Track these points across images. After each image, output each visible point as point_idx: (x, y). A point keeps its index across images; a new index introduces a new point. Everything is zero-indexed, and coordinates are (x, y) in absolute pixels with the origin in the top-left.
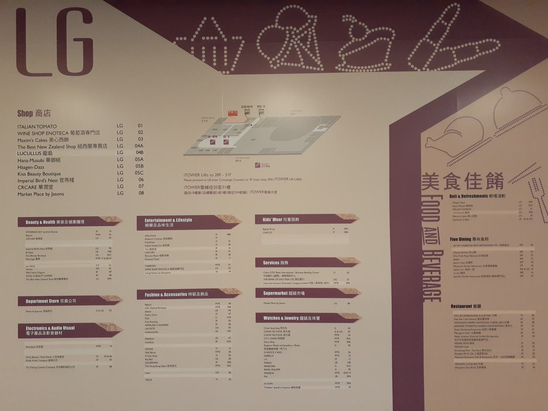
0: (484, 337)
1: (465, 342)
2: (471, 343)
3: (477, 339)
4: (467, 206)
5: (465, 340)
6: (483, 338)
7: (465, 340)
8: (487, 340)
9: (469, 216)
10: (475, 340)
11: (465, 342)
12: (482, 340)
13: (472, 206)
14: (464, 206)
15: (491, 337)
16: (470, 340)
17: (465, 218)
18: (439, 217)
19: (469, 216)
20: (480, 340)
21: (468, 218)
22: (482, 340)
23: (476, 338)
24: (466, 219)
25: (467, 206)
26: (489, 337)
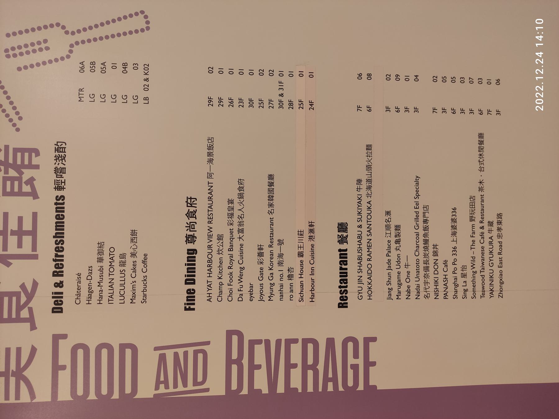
4: (100, 260)
13: (101, 245)
14: (101, 270)
18: (123, 347)
25: (100, 260)
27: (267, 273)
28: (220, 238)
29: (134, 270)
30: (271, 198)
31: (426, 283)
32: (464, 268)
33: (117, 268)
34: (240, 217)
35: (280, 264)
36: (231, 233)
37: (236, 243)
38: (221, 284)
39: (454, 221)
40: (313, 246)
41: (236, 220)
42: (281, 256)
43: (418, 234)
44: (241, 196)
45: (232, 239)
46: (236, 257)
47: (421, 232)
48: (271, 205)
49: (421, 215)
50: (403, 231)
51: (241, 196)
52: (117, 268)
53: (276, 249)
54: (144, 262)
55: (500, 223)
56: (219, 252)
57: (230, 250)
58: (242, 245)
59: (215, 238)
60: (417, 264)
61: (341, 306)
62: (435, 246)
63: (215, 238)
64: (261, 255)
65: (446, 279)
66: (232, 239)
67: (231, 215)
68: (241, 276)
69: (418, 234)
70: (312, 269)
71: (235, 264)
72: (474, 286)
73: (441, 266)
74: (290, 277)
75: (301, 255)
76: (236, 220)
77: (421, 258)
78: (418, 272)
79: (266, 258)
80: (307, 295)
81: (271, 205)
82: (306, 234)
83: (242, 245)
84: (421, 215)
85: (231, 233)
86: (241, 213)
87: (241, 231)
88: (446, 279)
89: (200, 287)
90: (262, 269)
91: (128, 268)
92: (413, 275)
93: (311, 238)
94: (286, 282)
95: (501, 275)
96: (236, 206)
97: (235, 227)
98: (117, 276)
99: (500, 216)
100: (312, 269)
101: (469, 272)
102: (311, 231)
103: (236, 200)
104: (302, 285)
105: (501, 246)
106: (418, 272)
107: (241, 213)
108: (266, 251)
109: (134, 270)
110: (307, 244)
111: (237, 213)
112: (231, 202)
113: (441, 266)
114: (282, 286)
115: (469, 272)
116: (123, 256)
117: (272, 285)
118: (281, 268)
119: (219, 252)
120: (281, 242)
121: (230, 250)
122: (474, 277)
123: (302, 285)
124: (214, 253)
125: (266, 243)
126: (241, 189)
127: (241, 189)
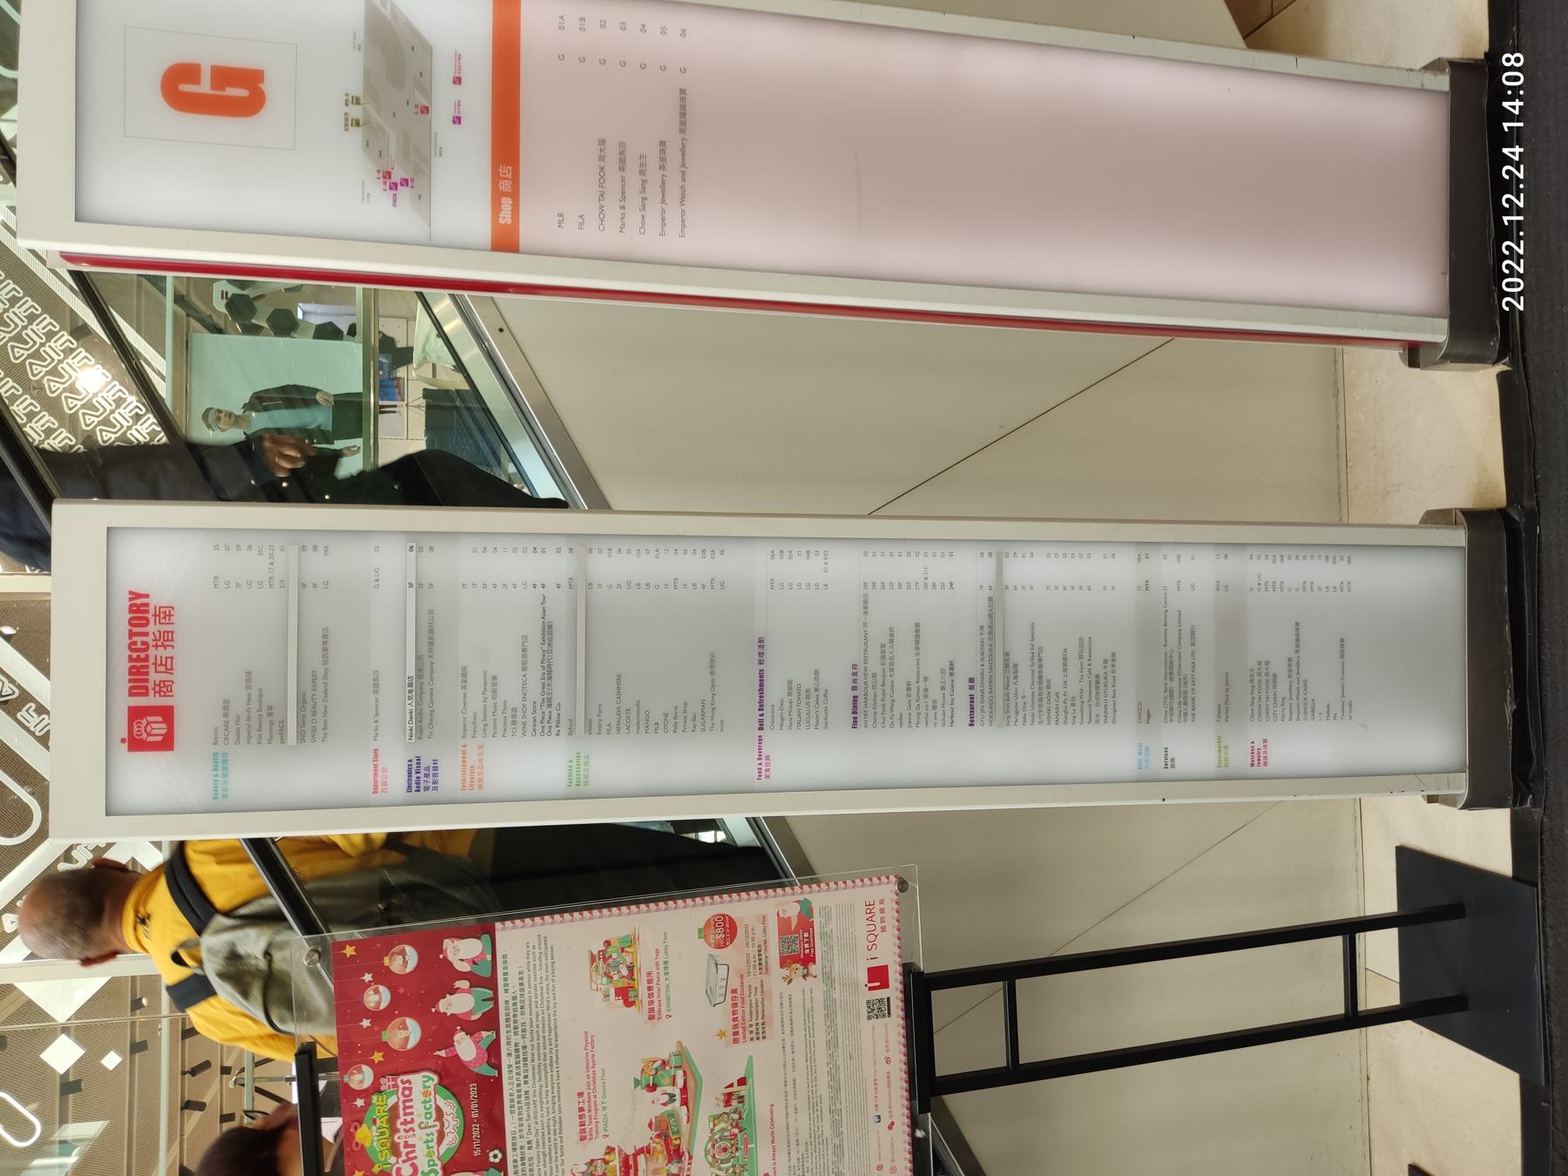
0: (1033, 656)
1: (1045, 700)
2: (1048, 687)
3: (1040, 672)
5: (1041, 700)
6: (1036, 658)
7: (1041, 700)
8: (1041, 649)
9: (816, 690)
10: (1040, 677)
11: (1045, 700)
12: (1040, 660)
15: (1033, 639)
16: (1040, 688)
17: (822, 698)
19: (816, 690)
20: (1040, 666)
21: (821, 693)
22: (1040, 660)
23: (1036, 674)
24: (825, 696)
26: (1033, 645)
27: (914, 704)
28: (874, 675)
29: (817, 702)
30: (917, 642)
31: (1040, 711)
32: (1073, 699)
33: (804, 701)
34: (890, 658)
35: (926, 696)
36: (884, 672)
37: (888, 680)
38: (875, 713)
39: (1065, 659)
40: (953, 681)
41: (887, 661)
42: (926, 690)
43: (1033, 672)
44: (891, 641)
45: (884, 676)
46: (888, 692)
47: (1036, 669)
48: (917, 648)
49: (1036, 655)
50: (1020, 669)
51: (891, 641)
52: (804, 701)
53: (922, 685)
54: (825, 696)
55: (1113, 660)
56: (874, 687)
57: (883, 685)
58: (892, 682)
59: (870, 676)
60: (1033, 695)
61: (971, 725)
62: (1048, 681)
63: (870, 676)
64: (909, 689)
65: (1057, 708)
66: (884, 676)
67: (883, 657)
68: (892, 706)
69: (1033, 672)
70: (952, 700)
71: (887, 697)
72: (1082, 713)
73: (1053, 697)
74: (934, 707)
75: (943, 688)
76: (887, 661)
77: (1036, 691)
78: (1033, 703)
79: (914, 692)
80: (948, 720)
81: (917, 648)
82: (948, 672)
83: (892, 682)
84: (1036, 655)
85: (884, 672)
86: (891, 655)
87: (892, 670)
88: (1057, 708)
89: (860, 716)
90: (910, 701)
91: (813, 700)
92: (1029, 705)
93: (951, 674)
94: (931, 712)
95: (1115, 704)
96: (888, 650)
97: (887, 667)
98: (803, 705)
99: (1113, 654)
100: (952, 700)
101: (1078, 702)
102: (952, 669)
103: (888, 645)
104: (944, 714)
105: (1114, 680)
106: (1033, 703)
107: (891, 655)
108: (914, 687)
109: (817, 702)
110: (948, 679)
111: (888, 655)
112: (883, 646)
113: (1053, 697)
114: (927, 715)
115: (1078, 702)
116: (808, 691)
117: (919, 714)
118: (926, 700)
119: (874, 687)
120: (926, 679)
121: (883, 685)
122: (1082, 706)
123: (944, 714)
124: (870, 687)
125: (913, 680)
126: (891, 635)
127: (891, 635)
